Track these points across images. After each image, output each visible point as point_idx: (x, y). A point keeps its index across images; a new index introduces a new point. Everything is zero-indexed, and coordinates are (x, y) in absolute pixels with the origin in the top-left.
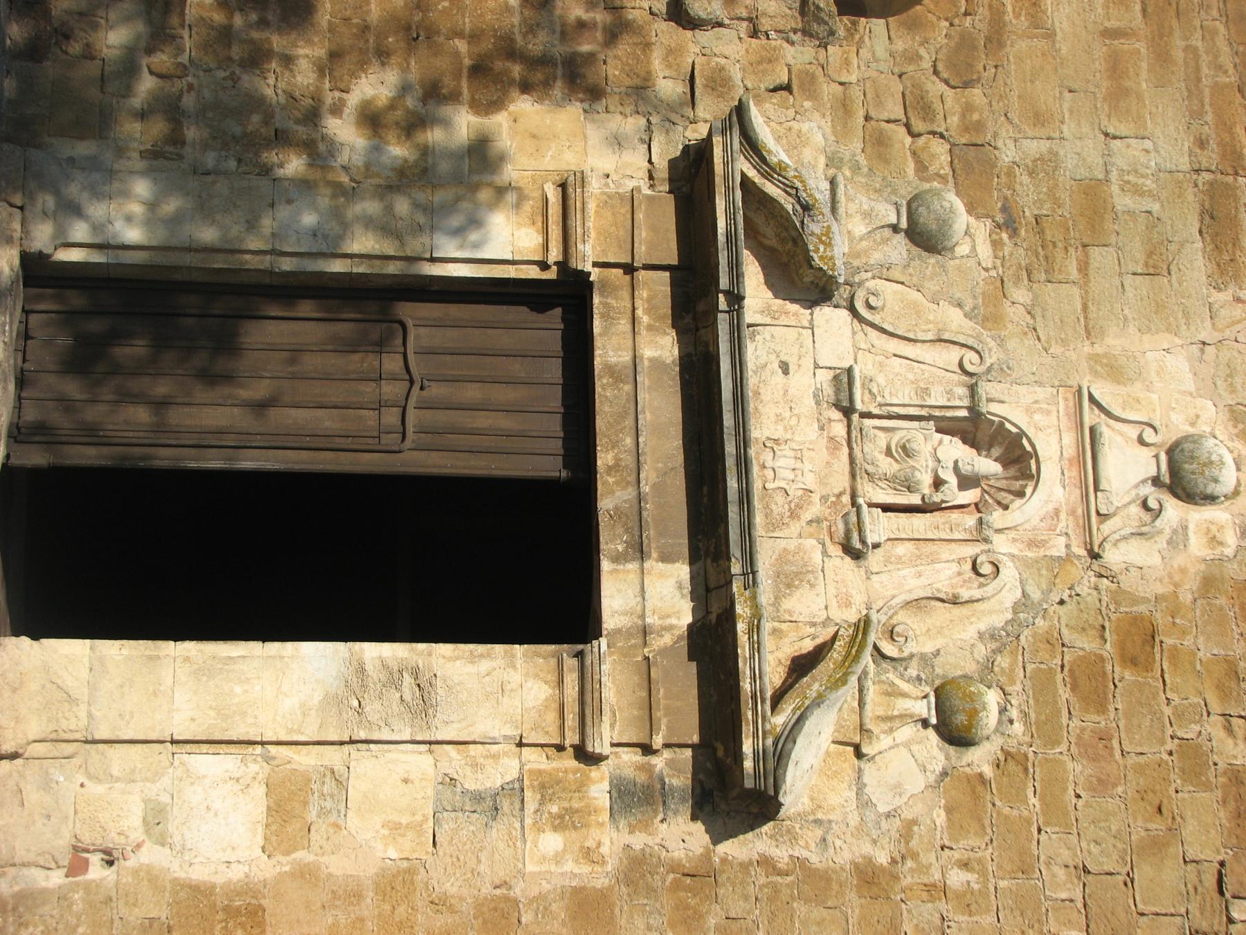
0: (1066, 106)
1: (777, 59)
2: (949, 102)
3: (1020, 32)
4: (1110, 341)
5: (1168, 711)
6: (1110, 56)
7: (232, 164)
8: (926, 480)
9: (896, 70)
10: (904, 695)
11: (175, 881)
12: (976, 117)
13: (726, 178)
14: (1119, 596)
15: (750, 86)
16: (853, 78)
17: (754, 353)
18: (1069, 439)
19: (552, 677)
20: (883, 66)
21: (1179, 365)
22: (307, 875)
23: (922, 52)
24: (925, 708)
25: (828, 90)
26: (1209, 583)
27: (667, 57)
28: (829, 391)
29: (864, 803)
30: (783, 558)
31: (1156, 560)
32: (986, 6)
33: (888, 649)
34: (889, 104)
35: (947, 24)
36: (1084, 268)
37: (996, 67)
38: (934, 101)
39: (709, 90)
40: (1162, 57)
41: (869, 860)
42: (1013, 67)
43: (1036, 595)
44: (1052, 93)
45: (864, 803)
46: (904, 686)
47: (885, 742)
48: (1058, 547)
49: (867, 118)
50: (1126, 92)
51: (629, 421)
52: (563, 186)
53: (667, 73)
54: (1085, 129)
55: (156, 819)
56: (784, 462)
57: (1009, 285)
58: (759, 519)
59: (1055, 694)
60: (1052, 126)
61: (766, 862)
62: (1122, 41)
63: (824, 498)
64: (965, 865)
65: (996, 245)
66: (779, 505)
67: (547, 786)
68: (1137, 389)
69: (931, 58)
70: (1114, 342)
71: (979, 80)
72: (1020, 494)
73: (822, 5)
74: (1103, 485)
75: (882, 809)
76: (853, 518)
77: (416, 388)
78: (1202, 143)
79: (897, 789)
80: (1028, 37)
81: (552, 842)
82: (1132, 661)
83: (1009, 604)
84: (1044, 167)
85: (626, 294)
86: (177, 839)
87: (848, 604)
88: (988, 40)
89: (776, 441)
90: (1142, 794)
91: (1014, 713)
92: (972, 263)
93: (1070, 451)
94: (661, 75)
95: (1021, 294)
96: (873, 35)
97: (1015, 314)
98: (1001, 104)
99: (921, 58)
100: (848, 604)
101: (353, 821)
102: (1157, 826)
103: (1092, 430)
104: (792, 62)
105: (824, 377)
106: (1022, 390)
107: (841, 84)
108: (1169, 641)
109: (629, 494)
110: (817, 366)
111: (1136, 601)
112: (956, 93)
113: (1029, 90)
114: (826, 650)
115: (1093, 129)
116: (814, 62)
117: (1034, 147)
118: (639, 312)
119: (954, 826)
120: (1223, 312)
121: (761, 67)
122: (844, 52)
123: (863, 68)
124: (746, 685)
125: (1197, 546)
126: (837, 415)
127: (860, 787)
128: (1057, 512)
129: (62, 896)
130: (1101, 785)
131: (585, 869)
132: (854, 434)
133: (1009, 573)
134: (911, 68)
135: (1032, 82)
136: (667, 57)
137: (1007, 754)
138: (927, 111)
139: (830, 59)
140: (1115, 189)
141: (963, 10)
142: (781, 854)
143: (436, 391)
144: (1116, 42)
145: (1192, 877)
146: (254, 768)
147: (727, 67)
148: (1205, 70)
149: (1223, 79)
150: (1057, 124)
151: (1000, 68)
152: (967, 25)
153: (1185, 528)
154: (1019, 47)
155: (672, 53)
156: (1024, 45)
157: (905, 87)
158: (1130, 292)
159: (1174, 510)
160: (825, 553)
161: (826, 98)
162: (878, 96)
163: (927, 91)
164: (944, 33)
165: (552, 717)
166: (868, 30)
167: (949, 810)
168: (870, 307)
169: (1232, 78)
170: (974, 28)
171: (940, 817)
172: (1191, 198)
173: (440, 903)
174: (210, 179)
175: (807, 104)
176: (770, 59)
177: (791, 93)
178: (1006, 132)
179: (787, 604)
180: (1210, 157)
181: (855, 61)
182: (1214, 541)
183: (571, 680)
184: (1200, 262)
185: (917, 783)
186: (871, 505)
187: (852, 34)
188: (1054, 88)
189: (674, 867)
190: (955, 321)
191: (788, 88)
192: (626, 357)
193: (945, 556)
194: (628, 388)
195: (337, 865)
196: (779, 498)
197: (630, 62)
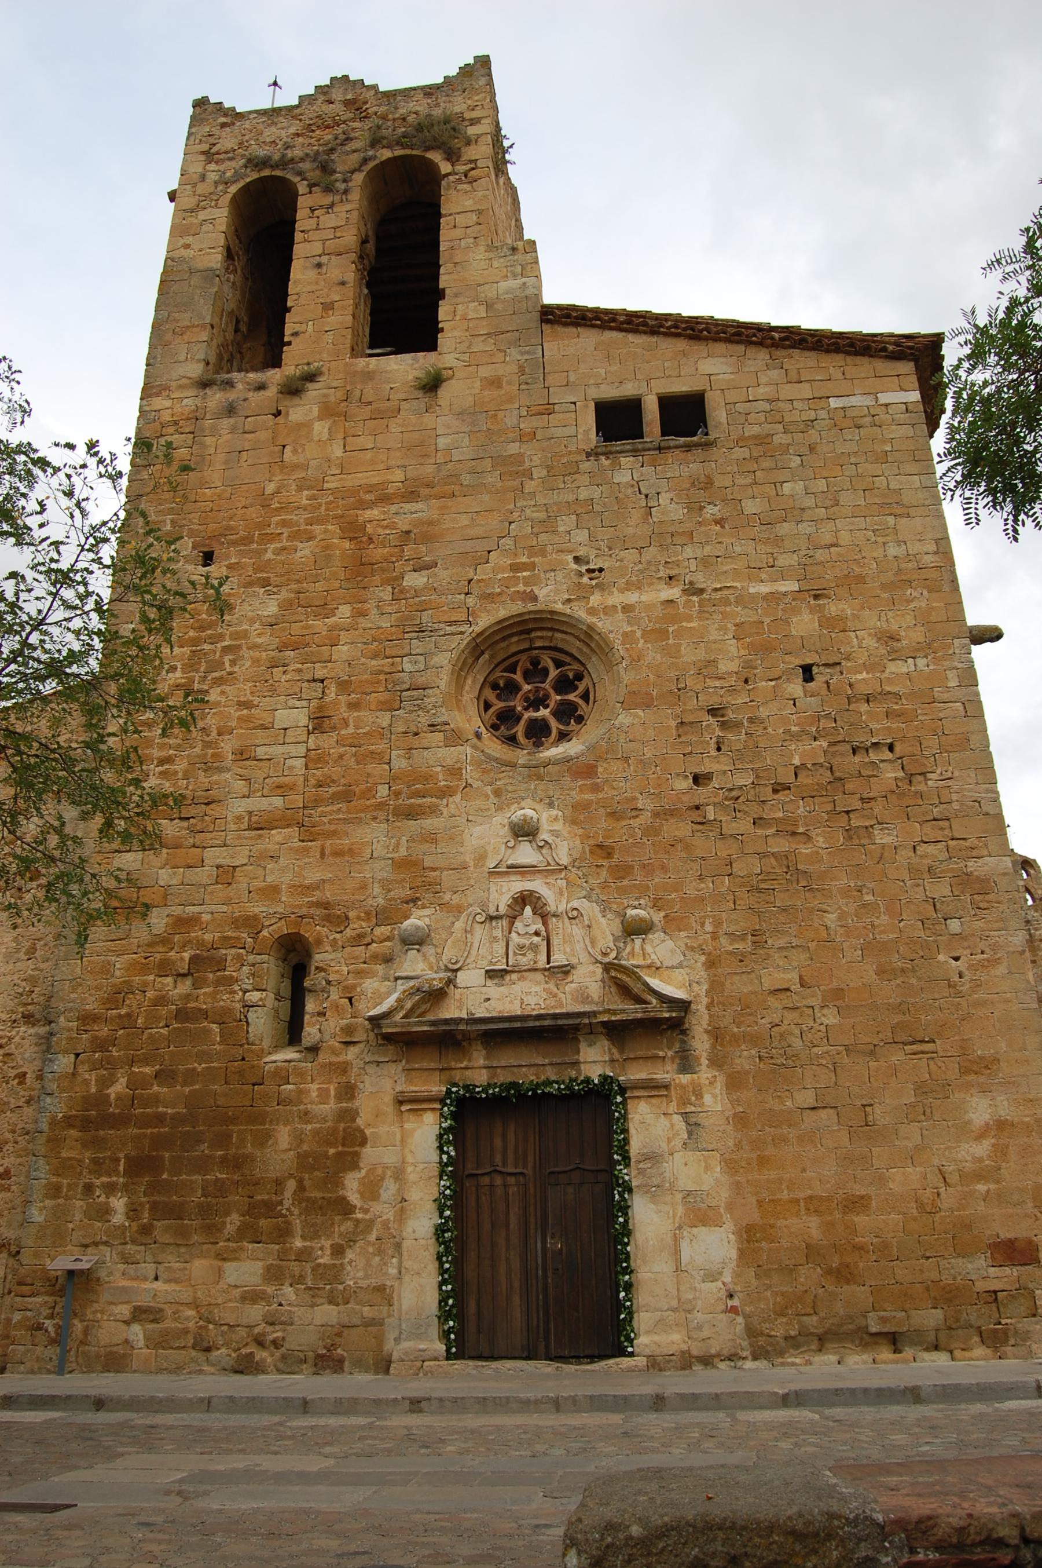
2: (356, 926)
4: (468, 859)
5: (630, 841)
7: (394, 1260)
8: (536, 939)
10: (633, 949)
11: (738, 1266)
12: (362, 915)
13: (403, 1026)
16: (345, 969)
17: (480, 1013)
18: (513, 878)
19: (636, 1101)
20: (340, 955)
21: (477, 830)
22: (730, 1207)
23: (331, 938)
24: (638, 942)
26: (574, 822)
28: (496, 981)
29: (680, 966)
30: (575, 1000)
31: (565, 842)
33: (613, 955)
34: (357, 953)
36: (434, 869)
40: (334, 834)
41: (704, 964)
43: (584, 893)
45: (680, 966)
46: (628, 949)
47: (653, 956)
48: (563, 883)
49: (365, 963)
50: (350, 849)
51: (515, 1070)
52: (401, 1103)
54: (367, 867)
55: (712, 1276)
56: (532, 1000)
57: (443, 902)
59: (627, 886)
61: (708, 1008)
63: (547, 983)
64: (703, 924)
65: (424, 907)
66: (552, 1002)
67: (684, 1102)
68: (490, 848)
70: (469, 859)
72: (539, 898)
74: (535, 863)
75: (682, 958)
76: (556, 970)
77: (498, 1168)
78: (375, 818)
79: (673, 952)
81: (708, 1099)
82: (609, 856)
83: (589, 904)
84: (386, 886)
85: (454, 1072)
86: (720, 1266)
87: (594, 972)
88: (326, 908)
89: (522, 1004)
91: (636, 903)
92: (433, 917)
93: (519, 877)
95: (447, 897)
97: (456, 899)
100: (594, 972)
101: (705, 1187)
102: (679, 847)
103: (508, 867)
105: (489, 983)
106: (491, 897)
108: (601, 839)
109: (549, 1069)
110: (485, 986)
111: (584, 852)
114: (619, 982)
117: (377, 890)
118: (462, 1065)
119: (687, 927)
120: (453, 812)
124: (639, 1015)
125: (558, 826)
126: (507, 978)
127: (673, 967)
128: (546, 883)
129: (746, 1317)
130: (664, 868)
131: (718, 1085)
132: (516, 969)
133: (575, 904)
137: (654, 906)
138: (360, 936)
140: (396, 855)
142: (705, 1001)
143: (498, 1159)
145: (699, 834)
146: (685, 1233)
148: (341, 816)
149: (344, 809)
153: (551, 831)
154: (328, 894)
155: (334, 1052)
158: (444, 850)
159: (544, 835)
160: (572, 982)
165: (654, 1101)
167: (680, 930)
168: (456, 963)
169: (343, 806)
171: (683, 934)
172: (399, 824)
173: (738, 1146)
174: (403, 1270)
175: (358, 990)
176: (337, 1007)
178: (370, 901)
179: (596, 999)
180: (381, 815)
182: (556, 819)
183: (636, 1094)
184: (429, 821)
185: (670, 944)
186: (548, 963)
189: (713, 1047)
190: (459, 925)
191: (350, 999)
192: (484, 1071)
193: (569, 931)
194: (499, 1070)
195: (725, 1194)
196: (548, 1002)
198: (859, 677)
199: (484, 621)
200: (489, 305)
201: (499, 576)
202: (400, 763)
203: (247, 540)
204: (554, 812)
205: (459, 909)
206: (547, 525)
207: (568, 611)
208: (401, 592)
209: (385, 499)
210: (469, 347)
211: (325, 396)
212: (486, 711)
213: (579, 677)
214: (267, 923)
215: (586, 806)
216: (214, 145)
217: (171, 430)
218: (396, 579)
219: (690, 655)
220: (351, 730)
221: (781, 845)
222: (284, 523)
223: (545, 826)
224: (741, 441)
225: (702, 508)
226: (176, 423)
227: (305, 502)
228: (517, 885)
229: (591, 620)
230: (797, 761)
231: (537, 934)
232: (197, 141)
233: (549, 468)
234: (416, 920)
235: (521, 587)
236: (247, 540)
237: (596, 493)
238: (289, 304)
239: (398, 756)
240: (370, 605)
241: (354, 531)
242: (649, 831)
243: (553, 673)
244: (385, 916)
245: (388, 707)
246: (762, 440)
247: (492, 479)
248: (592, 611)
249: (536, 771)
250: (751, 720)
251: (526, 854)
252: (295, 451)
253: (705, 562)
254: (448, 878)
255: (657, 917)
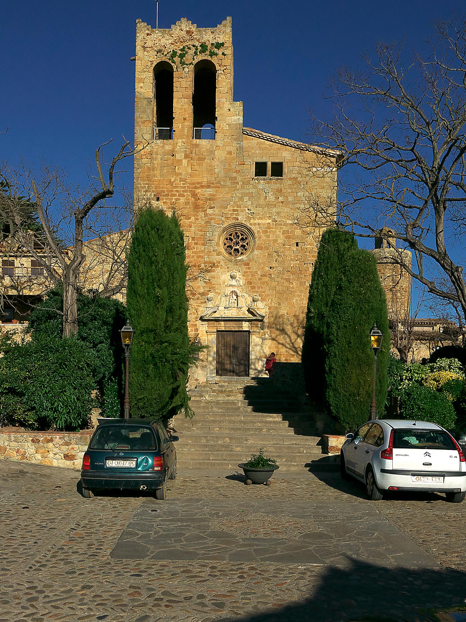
14: (245, 284)
18: (230, 287)
21: (223, 276)
25: (197, 307)
36: (214, 284)
58: (239, 317)
64: (269, 300)
65: (212, 292)
66: (238, 314)
68: (226, 280)
90: (263, 284)
95: (217, 291)
97: (219, 291)
117: (202, 288)
125: (241, 276)
130: (262, 288)
133: (243, 294)
138: (198, 298)
159: (237, 278)
173: (271, 344)
176: (194, 313)
190: (219, 297)
198: (308, 246)
199: (226, 225)
200: (229, 125)
201: (230, 212)
202: (206, 259)
203: (167, 195)
204: (240, 273)
205: (219, 294)
206: (241, 199)
207: (245, 224)
208: (206, 214)
209: (202, 187)
210: (223, 140)
211: (186, 151)
212: (225, 245)
213: (246, 238)
215: (247, 272)
216: (146, 43)
217: (145, 157)
218: (205, 210)
219: (272, 237)
220: (195, 250)
221: (286, 284)
222: (177, 191)
223: (238, 276)
224: (290, 179)
225: (279, 198)
226: (145, 155)
227: (182, 185)
228: (232, 289)
229: (250, 226)
230: (292, 266)
231: (235, 300)
232: (140, 41)
233: (243, 182)
234: (210, 295)
235: (235, 216)
236: (167, 195)
237: (254, 191)
238: (174, 116)
239: (206, 257)
240: (199, 217)
241: (194, 195)
242: (259, 279)
243: (241, 237)
244: (203, 294)
245: (203, 244)
246: (295, 179)
247: (229, 183)
248: (251, 224)
249: (236, 262)
250: (284, 255)
251: (234, 282)
252: (178, 169)
253: (278, 213)
254: (217, 286)
255: (260, 298)
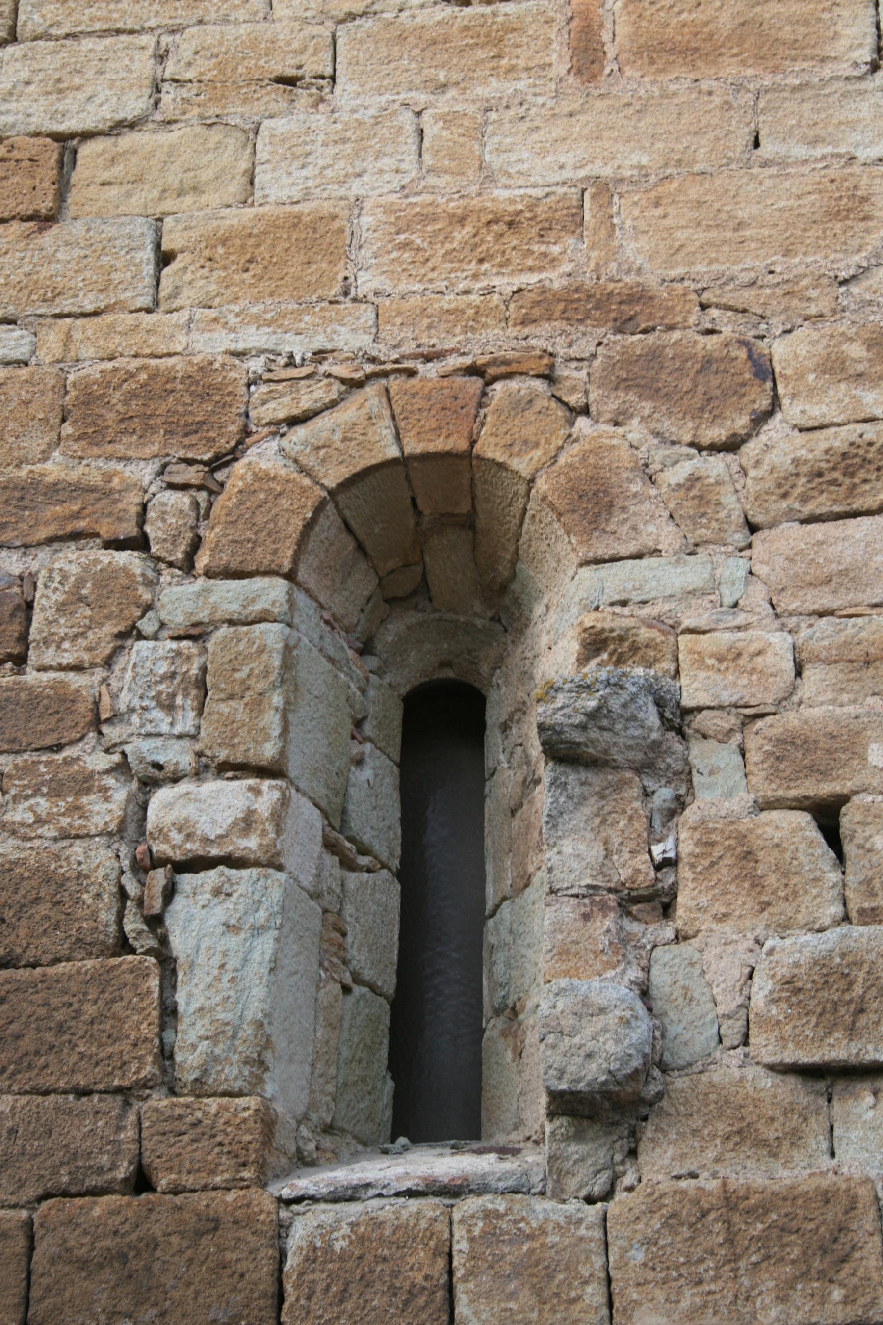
0: (800, 151)
1: (742, 838)
2: (817, 411)
3: (594, 254)
6: (652, 62)
9: (740, 537)
12: (856, 350)
15: (836, 910)
20: (737, 568)
23: (677, 475)
27: (763, 1143)
32: (527, 331)
35: (582, 422)
37: (704, 307)
38: (824, 446)
39: (862, 1021)
42: (701, 268)
44: (768, 183)
53: (817, 1143)
60: (865, 180)
62: (606, 37)
69: (690, 457)
71: (742, 343)
73: (592, 704)
80: (611, 236)
94: (826, 1162)
96: (636, 597)
98: (813, 293)
99: (694, 480)
104: (742, 800)
107: (799, 673)
112: (794, 396)
113: (766, 232)
115: (862, 93)
116: (737, 738)
121: (772, 880)
122: (700, 661)
123: (741, 619)
134: (729, 500)
135: (740, 226)
136: (763, 1143)
139: (727, 697)
141: (539, 385)
144: (611, 50)
147: (783, 971)
150: (856, 169)
151: (706, 297)
152: (583, 374)
156: (633, 245)
157: (790, 515)
161: (851, 709)
162: (828, 581)
163: (796, 462)
164: (610, 429)
166: (617, 609)
170: (594, 356)
177: (843, 799)
181: (725, 638)
187: (635, 648)
188: (752, 177)
197: (795, 1253)
214: (280, 409)
